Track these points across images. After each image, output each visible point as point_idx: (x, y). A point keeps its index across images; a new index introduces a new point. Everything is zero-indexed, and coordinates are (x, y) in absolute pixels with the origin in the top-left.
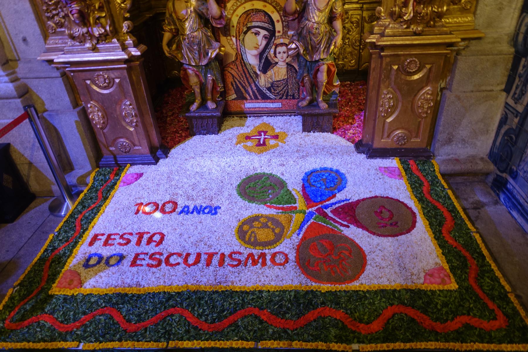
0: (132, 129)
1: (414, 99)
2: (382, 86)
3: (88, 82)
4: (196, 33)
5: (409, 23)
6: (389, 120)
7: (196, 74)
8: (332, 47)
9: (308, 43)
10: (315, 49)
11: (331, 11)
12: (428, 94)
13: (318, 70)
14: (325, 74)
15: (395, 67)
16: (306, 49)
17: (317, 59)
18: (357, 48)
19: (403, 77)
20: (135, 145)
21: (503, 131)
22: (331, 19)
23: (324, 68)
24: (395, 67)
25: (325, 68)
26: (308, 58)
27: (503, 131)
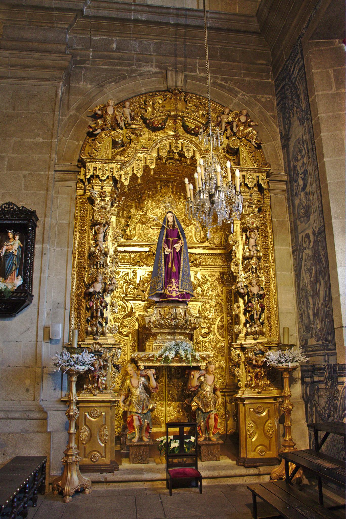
0: (103, 445)
1: (264, 427)
2: (247, 420)
3: (86, 413)
4: (143, 395)
5: (254, 388)
6: (253, 440)
7: (139, 419)
8: (217, 404)
9: (203, 402)
10: (208, 406)
11: (215, 387)
12: (270, 424)
13: (209, 418)
14: (213, 420)
15: (252, 410)
16: (203, 406)
17: (209, 411)
18: (224, 420)
19: (256, 414)
20: (102, 457)
21: (311, 443)
22: (215, 391)
23: (213, 416)
24: (252, 410)
25: (213, 416)
26: (204, 410)
27: (311, 443)
